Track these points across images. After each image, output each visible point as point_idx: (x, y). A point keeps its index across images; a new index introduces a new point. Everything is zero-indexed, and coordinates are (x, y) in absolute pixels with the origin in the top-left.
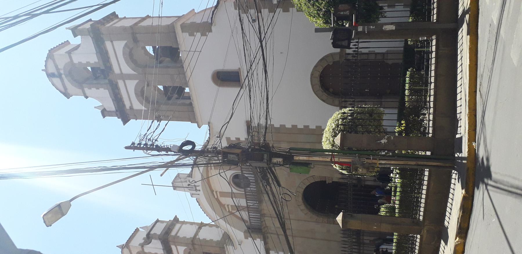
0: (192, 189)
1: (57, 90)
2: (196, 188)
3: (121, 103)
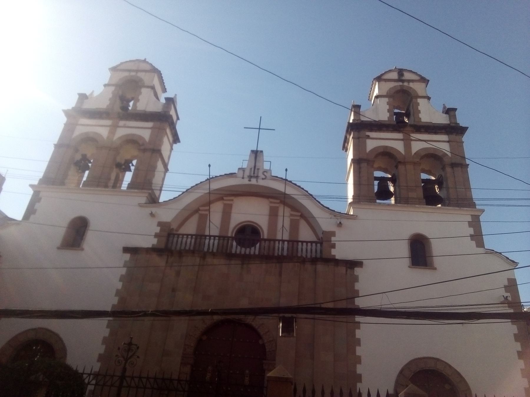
0: (252, 172)
1: (385, 72)
2: (254, 177)
3: (376, 129)
